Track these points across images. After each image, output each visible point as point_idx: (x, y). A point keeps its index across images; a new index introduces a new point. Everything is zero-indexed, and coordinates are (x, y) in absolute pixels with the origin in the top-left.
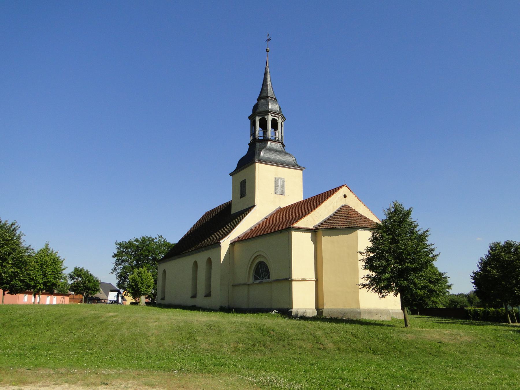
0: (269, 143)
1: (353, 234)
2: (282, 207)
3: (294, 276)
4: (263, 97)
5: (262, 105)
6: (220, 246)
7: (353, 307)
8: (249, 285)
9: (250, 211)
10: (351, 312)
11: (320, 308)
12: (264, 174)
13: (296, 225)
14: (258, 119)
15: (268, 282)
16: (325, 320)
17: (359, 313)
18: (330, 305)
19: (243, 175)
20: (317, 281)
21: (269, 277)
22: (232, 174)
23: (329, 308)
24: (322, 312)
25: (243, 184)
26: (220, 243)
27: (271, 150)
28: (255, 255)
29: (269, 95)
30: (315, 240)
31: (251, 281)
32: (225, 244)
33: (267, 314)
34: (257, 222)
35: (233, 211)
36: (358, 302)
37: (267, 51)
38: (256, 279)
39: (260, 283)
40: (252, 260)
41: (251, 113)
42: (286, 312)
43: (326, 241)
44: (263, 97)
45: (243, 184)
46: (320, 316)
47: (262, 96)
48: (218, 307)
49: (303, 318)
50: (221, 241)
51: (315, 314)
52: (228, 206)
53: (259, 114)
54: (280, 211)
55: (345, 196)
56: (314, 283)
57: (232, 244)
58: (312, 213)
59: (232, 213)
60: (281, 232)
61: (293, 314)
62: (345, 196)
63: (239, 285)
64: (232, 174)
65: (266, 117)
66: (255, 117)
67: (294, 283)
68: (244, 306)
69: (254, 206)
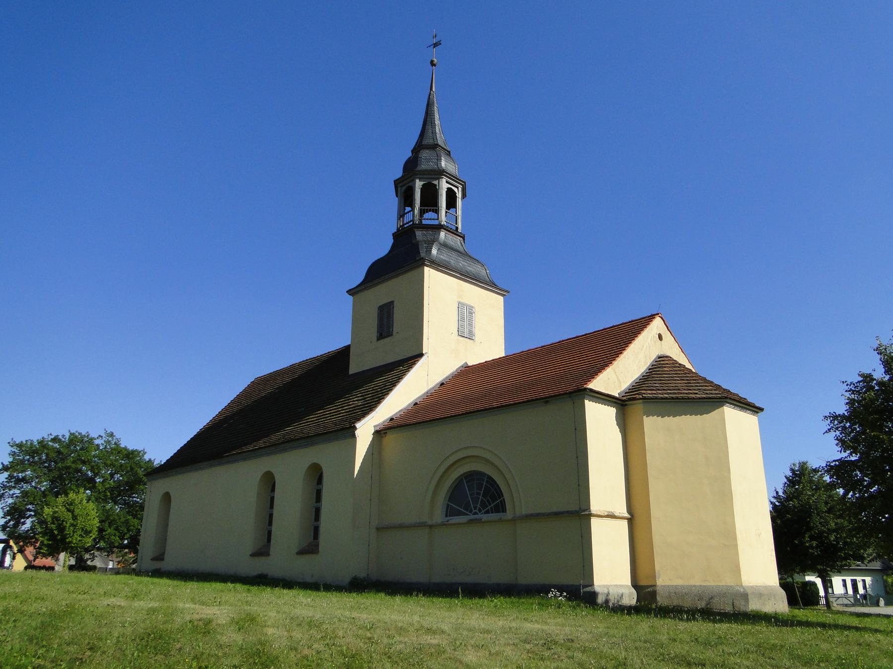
0: (443, 234)
1: (715, 414)
2: (471, 363)
3: (595, 507)
4: (425, 143)
5: (428, 160)
6: (354, 436)
7: (727, 581)
8: (431, 526)
9: (414, 364)
10: (724, 593)
11: (643, 582)
12: (442, 294)
13: (596, 384)
14: (419, 184)
15: (500, 520)
16: (665, 612)
17: (745, 596)
18: (668, 578)
19: (382, 293)
20: (631, 521)
21: (501, 508)
22: (351, 292)
23: (669, 583)
24: (654, 594)
25: (386, 313)
26: (355, 428)
27: (445, 246)
28: (470, 452)
29: (440, 143)
30: (623, 423)
31: (439, 516)
32: (365, 431)
33: (508, 599)
34: (425, 390)
35: (353, 370)
36: (736, 570)
37: (432, 64)
38: (450, 512)
39: (471, 522)
40: (442, 470)
41: (399, 173)
42: (582, 595)
43: (656, 428)
44: (425, 143)
45: (386, 313)
46: (648, 602)
47: (425, 142)
48: (347, 580)
49: (620, 609)
50: (358, 425)
51: (630, 598)
52: (342, 355)
53: (423, 174)
54: (467, 372)
55: (660, 337)
56: (625, 522)
57: (380, 433)
58: (615, 363)
59: (351, 372)
60: (547, 402)
61: (600, 600)
62: (660, 337)
63: (401, 527)
64: (351, 292)
65: (436, 182)
66: (413, 181)
67: (594, 521)
68: (413, 577)
69: (421, 355)
